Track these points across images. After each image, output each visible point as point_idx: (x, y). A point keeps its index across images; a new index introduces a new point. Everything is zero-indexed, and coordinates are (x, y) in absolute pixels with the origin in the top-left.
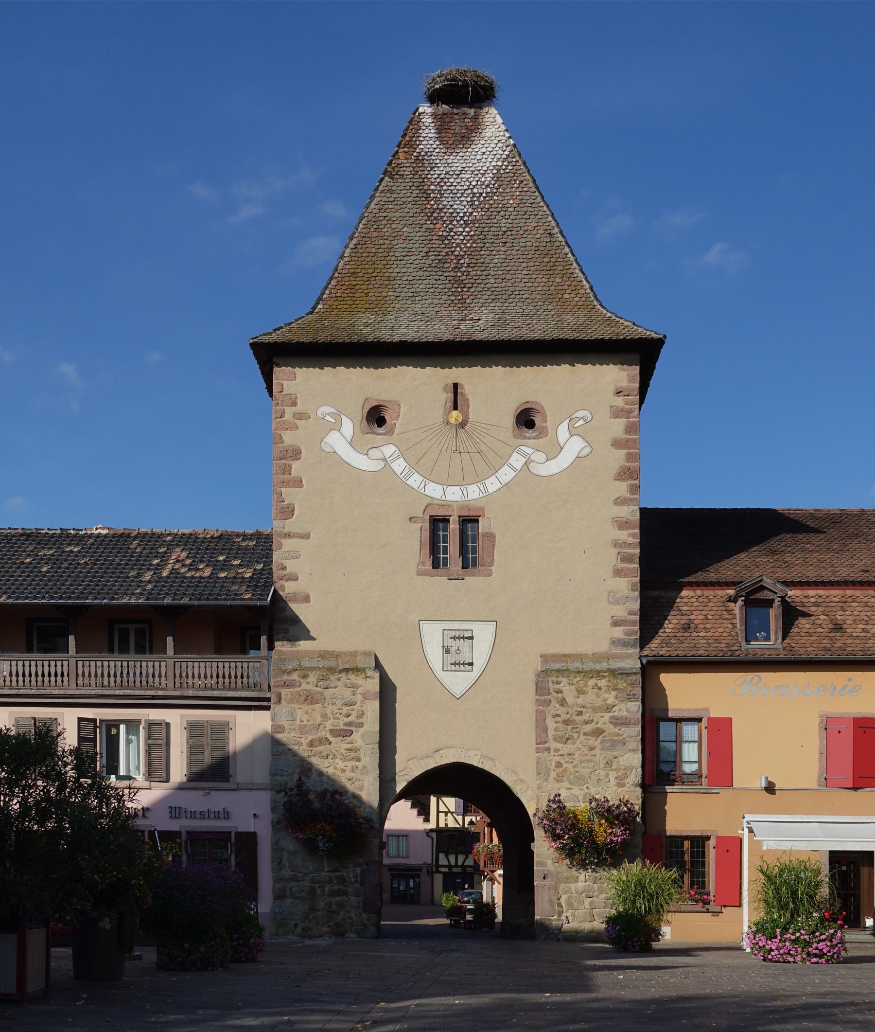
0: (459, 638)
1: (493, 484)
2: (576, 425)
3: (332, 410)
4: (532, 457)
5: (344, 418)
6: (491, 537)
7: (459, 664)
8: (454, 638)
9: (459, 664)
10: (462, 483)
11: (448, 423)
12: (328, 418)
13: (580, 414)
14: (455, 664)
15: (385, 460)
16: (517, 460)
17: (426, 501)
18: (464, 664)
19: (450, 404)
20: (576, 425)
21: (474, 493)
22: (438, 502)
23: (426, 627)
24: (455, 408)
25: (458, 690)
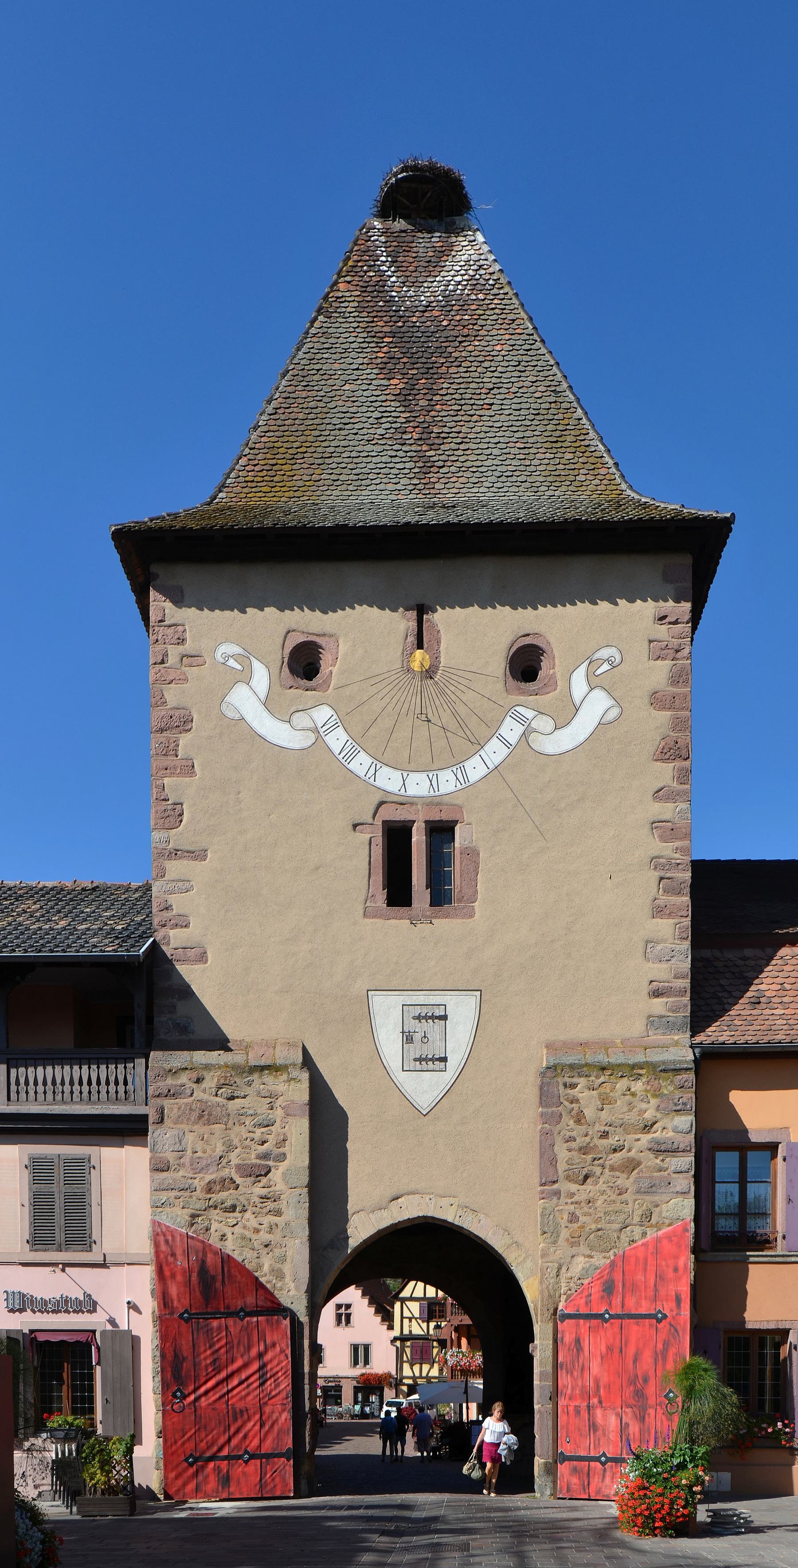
0: (426, 1018)
1: (475, 769)
4: (534, 725)
6: (472, 853)
8: (419, 1018)
12: (232, 663)
13: (605, 653)
21: (447, 782)
23: (378, 1001)
24: (420, 646)
25: (424, 1101)
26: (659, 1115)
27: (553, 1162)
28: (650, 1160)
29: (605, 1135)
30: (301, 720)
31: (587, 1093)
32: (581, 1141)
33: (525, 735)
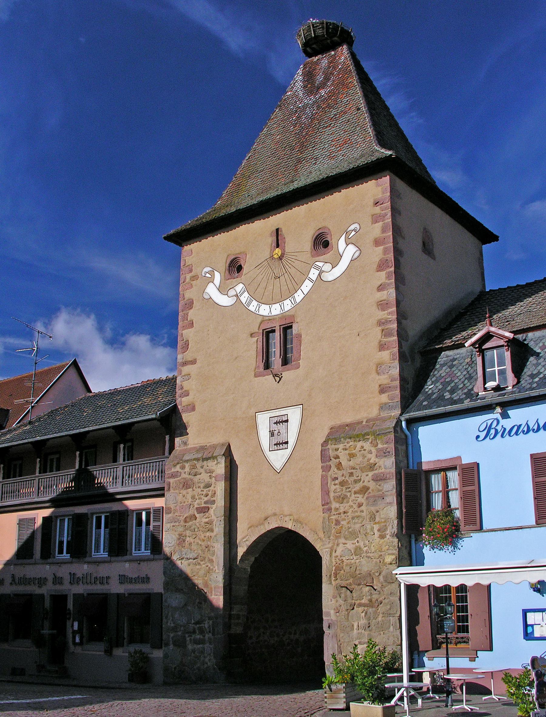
0: (279, 422)
1: (299, 296)
2: (350, 237)
3: (209, 269)
5: (216, 273)
6: (299, 336)
7: (279, 444)
8: (276, 423)
9: (279, 444)
12: (208, 275)
13: (352, 227)
16: (314, 274)
17: (260, 320)
18: (282, 443)
19: (274, 244)
20: (350, 237)
21: (288, 305)
22: (267, 318)
24: (278, 246)
26: (377, 460)
29: (351, 474)
30: (232, 292)
31: (343, 452)
32: (340, 479)
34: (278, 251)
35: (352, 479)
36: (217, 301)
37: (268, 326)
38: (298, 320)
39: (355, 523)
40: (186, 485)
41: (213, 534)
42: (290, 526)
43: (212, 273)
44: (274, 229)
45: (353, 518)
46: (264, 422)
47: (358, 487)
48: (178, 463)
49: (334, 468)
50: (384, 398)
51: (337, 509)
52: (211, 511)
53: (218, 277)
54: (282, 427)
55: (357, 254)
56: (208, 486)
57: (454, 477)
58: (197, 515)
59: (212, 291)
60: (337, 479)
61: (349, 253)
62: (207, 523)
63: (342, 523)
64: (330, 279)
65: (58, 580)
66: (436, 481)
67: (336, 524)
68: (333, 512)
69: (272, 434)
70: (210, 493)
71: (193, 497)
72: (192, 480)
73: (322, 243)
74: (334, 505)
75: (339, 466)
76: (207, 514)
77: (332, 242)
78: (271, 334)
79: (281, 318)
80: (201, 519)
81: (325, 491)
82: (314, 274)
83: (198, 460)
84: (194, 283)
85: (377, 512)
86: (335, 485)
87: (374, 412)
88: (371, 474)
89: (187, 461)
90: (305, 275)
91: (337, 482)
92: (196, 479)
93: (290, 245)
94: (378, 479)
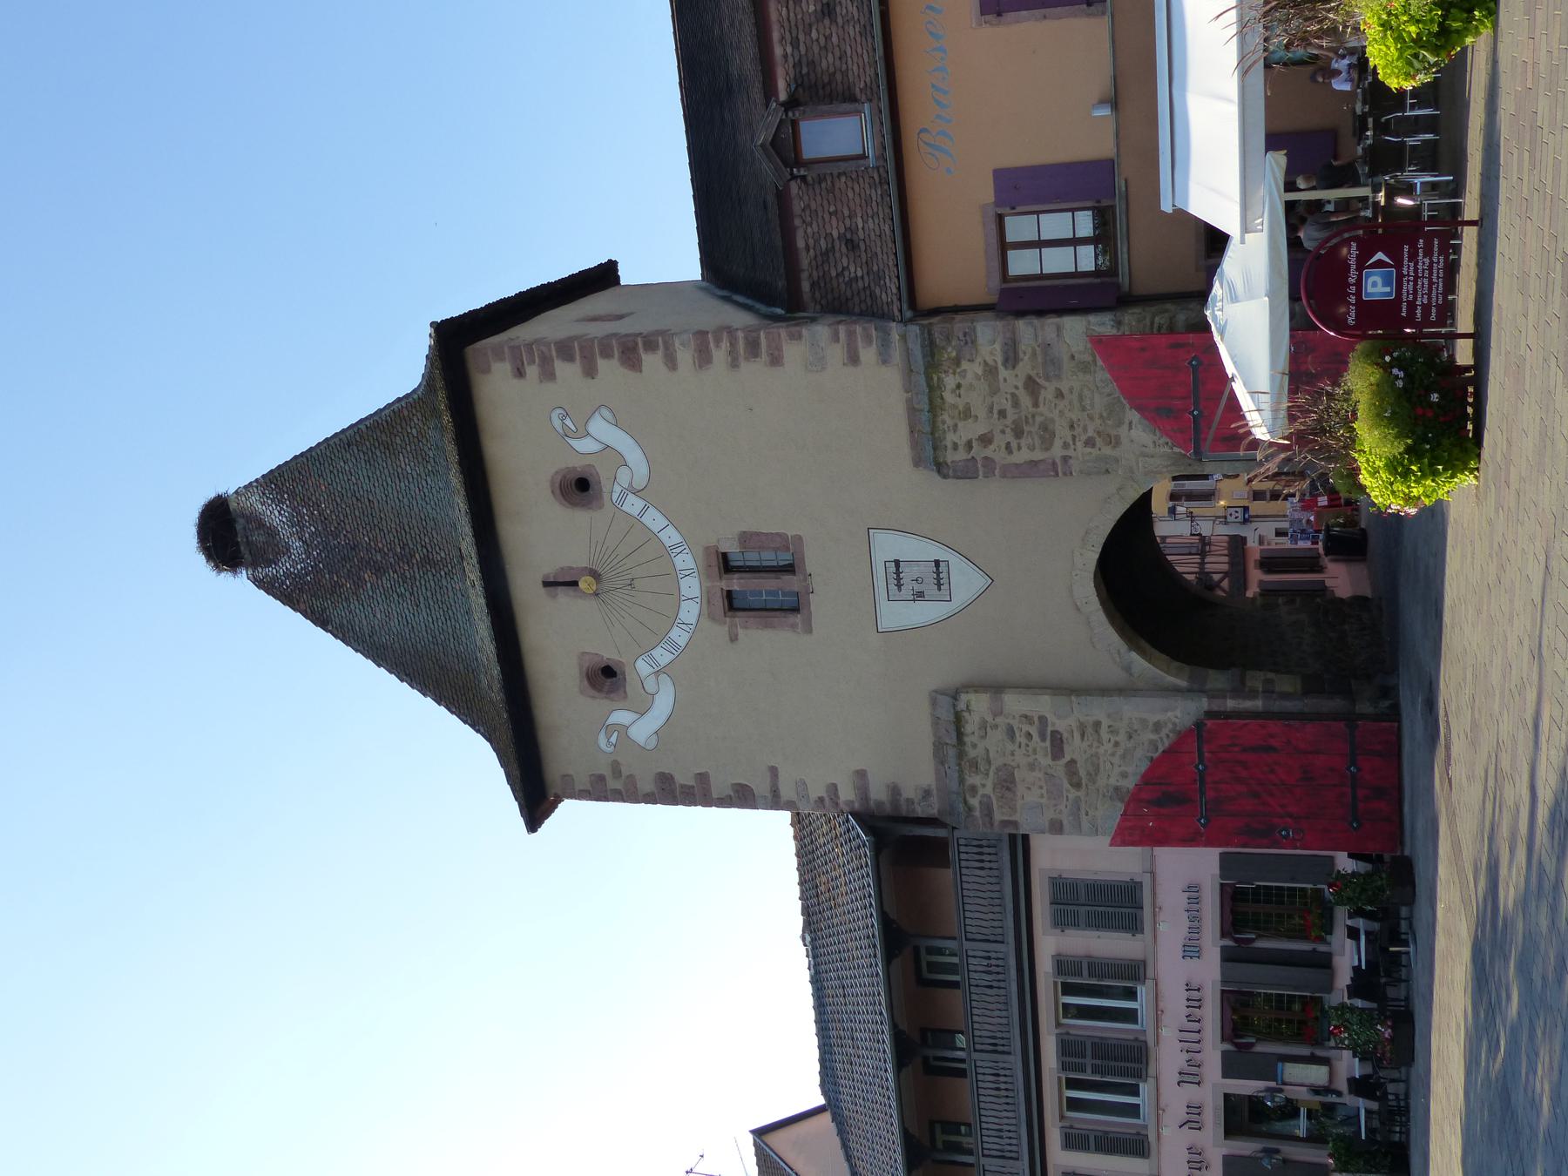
0: (899, 579)
1: (671, 537)
6: (746, 538)
7: (938, 579)
8: (899, 586)
9: (938, 579)
10: (673, 576)
11: (596, 594)
12: (613, 739)
13: (557, 423)
14: (939, 585)
15: (657, 673)
16: (633, 505)
18: (938, 573)
19: (570, 590)
22: (705, 606)
23: (885, 624)
24: (575, 584)
25: (978, 582)
26: (979, 359)
27: (1034, 464)
28: (1025, 368)
29: (1002, 414)
30: (650, 685)
32: (1009, 437)
33: (636, 493)
34: (585, 583)
35: (1010, 412)
36: (664, 718)
37: (719, 603)
38: (713, 542)
39: (1092, 405)
40: (1007, 783)
41: (1105, 723)
42: (1094, 556)
43: (610, 729)
44: (542, 590)
45: (1084, 409)
46: (899, 614)
47: (1025, 400)
48: (965, 802)
49: (988, 452)
50: (868, 354)
51: (1066, 446)
52: (1061, 725)
53: (621, 717)
54: (908, 574)
55: (605, 412)
56: (1011, 733)
57: (1019, 227)
58: (1067, 758)
59: (643, 730)
60: (1008, 444)
61: (603, 430)
62: (1083, 736)
63: (1090, 433)
64: (644, 470)
65: (1193, 1120)
66: (1022, 264)
67: (1094, 446)
68: (1070, 452)
69: (920, 595)
70: (1026, 728)
71: (1032, 767)
72: (998, 770)
73: (580, 488)
74: (1057, 451)
75: (986, 440)
76: (1065, 735)
77: (577, 463)
78: (736, 604)
79: (709, 576)
80: (1075, 748)
81: (1031, 469)
82: (633, 505)
83: (961, 755)
84: (625, 771)
85: (1073, 357)
86: (1019, 448)
87: (892, 377)
88: (1003, 373)
89: (962, 781)
90: (636, 522)
91: (1014, 445)
92: (997, 761)
93: (575, 557)
94: (1011, 358)
